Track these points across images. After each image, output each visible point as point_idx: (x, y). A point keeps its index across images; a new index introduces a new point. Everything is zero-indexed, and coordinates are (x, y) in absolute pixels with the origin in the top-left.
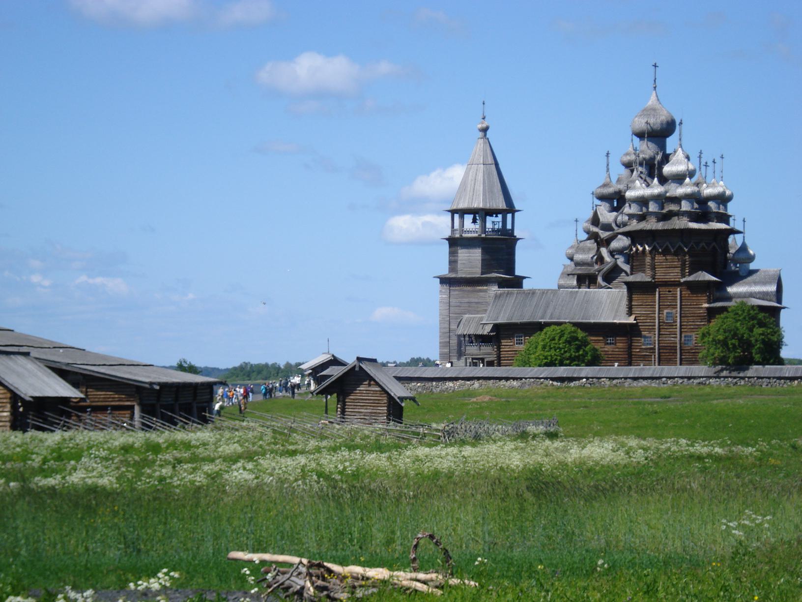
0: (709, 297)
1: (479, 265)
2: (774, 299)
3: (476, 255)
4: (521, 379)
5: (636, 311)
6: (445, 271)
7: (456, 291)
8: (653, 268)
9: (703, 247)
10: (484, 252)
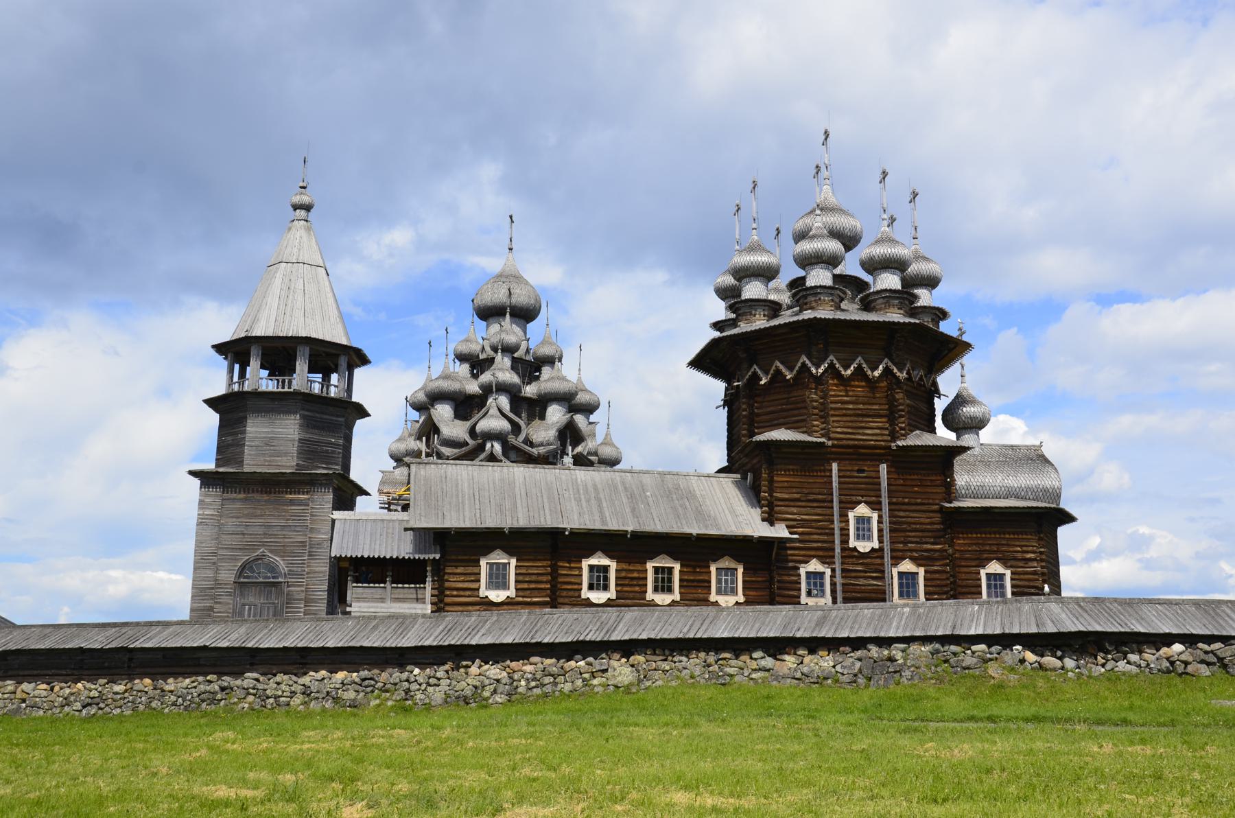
1: (294, 450)
4: (858, 643)
7: (237, 502)
10: (309, 424)
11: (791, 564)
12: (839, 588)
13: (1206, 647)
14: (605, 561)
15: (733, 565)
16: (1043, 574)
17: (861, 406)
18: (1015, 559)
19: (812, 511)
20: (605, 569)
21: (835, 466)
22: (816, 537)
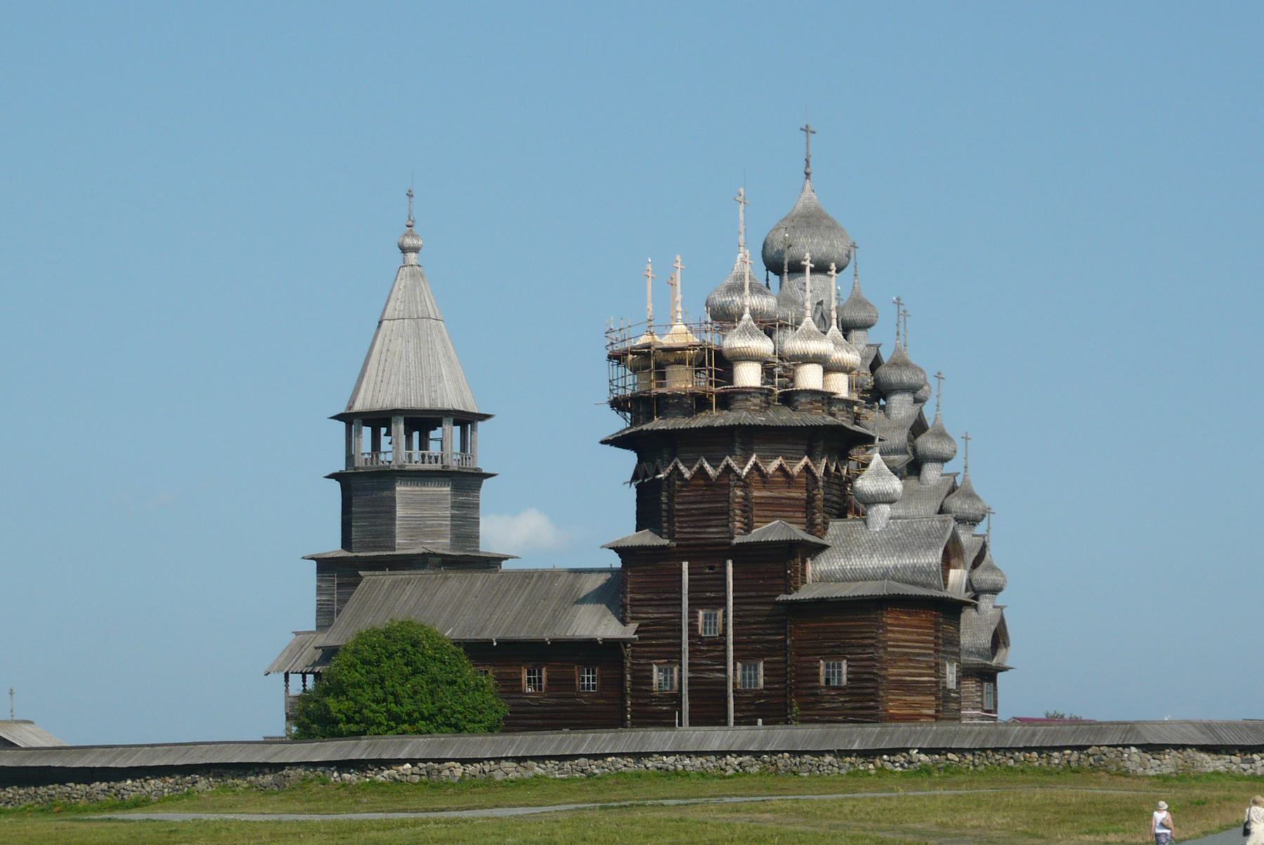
4: (281, 766)
6: (332, 545)
12: (685, 682)
13: (421, 765)
17: (707, 506)
21: (685, 565)
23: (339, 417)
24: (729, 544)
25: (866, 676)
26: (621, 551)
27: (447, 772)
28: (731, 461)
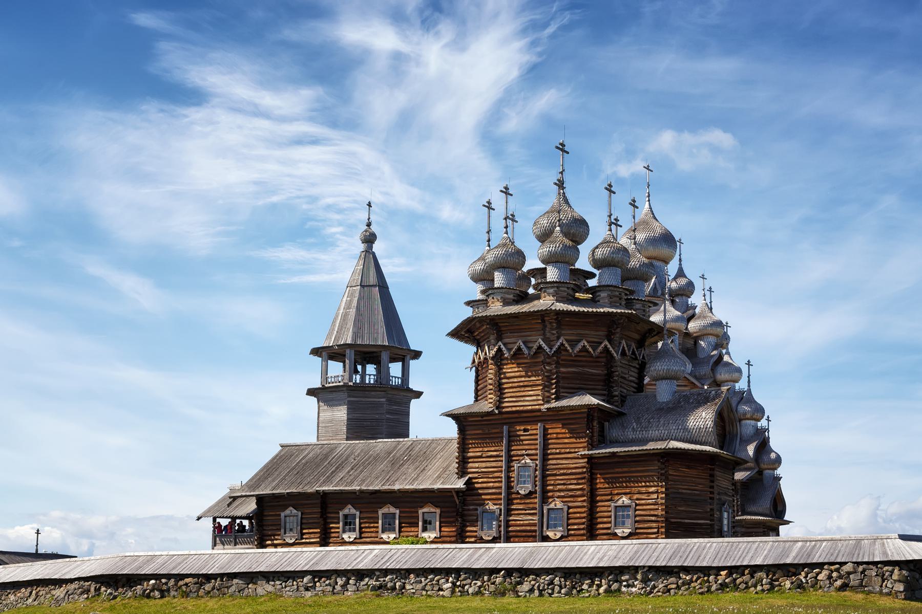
0: (591, 438)
1: (345, 428)
2: (712, 438)
3: (341, 413)
5: (473, 467)
8: (500, 389)
9: (584, 349)
11: (471, 507)
14: (353, 511)
15: (432, 510)
16: (662, 504)
18: (640, 493)
19: (488, 464)
20: (354, 516)
22: (491, 484)
23: (316, 352)
24: (539, 410)
25: (653, 518)
26: (460, 418)
27: (184, 588)
28: (542, 343)
